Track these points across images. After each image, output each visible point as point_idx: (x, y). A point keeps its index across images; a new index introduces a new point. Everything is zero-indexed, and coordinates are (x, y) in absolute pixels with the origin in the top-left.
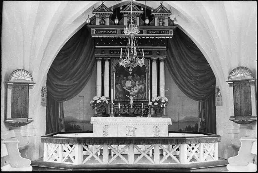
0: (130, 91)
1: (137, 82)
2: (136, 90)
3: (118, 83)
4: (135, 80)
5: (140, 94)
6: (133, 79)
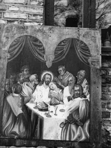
0: (44, 116)
1: (67, 91)
2: (63, 113)
3: (13, 90)
4: (63, 84)
5: (73, 127)
6: (54, 81)
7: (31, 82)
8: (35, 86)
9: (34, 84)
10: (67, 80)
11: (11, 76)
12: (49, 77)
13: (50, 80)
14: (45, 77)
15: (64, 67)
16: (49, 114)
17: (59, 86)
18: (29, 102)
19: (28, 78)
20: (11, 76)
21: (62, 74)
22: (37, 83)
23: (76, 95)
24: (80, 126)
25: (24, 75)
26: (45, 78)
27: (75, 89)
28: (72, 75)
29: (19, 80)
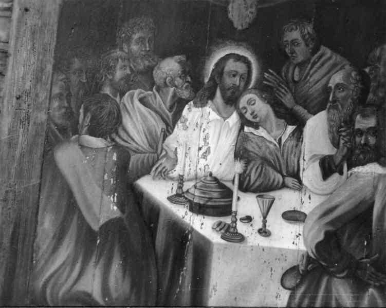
0: (215, 238)
2: (297, 228)
3: (84, 119)
6: (264, 89)
7: (158, 90)
8: (178, 105)
9: (174, 95)
10: (319, 86)
11: (77, 64)
12: (240, 67)
13: (242, 84)
14: (223, 69)
15: (309, 29)
16: (235, 228)
17: (286, 108)
18: (148, 173)
19: (149, 71)
20: (77, 64)
21: (300, 58)
22: (185, 94)
23: (362, 153)
24: (375, 287)
25: (130, 57)
26: (221, 74)
27: (357, 126)
28: (346, 62)
29: (108, 82)
